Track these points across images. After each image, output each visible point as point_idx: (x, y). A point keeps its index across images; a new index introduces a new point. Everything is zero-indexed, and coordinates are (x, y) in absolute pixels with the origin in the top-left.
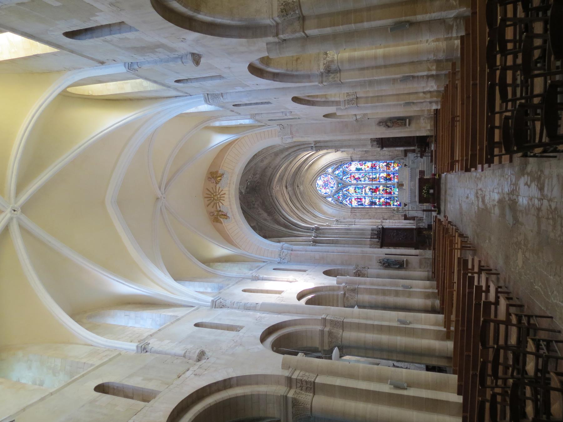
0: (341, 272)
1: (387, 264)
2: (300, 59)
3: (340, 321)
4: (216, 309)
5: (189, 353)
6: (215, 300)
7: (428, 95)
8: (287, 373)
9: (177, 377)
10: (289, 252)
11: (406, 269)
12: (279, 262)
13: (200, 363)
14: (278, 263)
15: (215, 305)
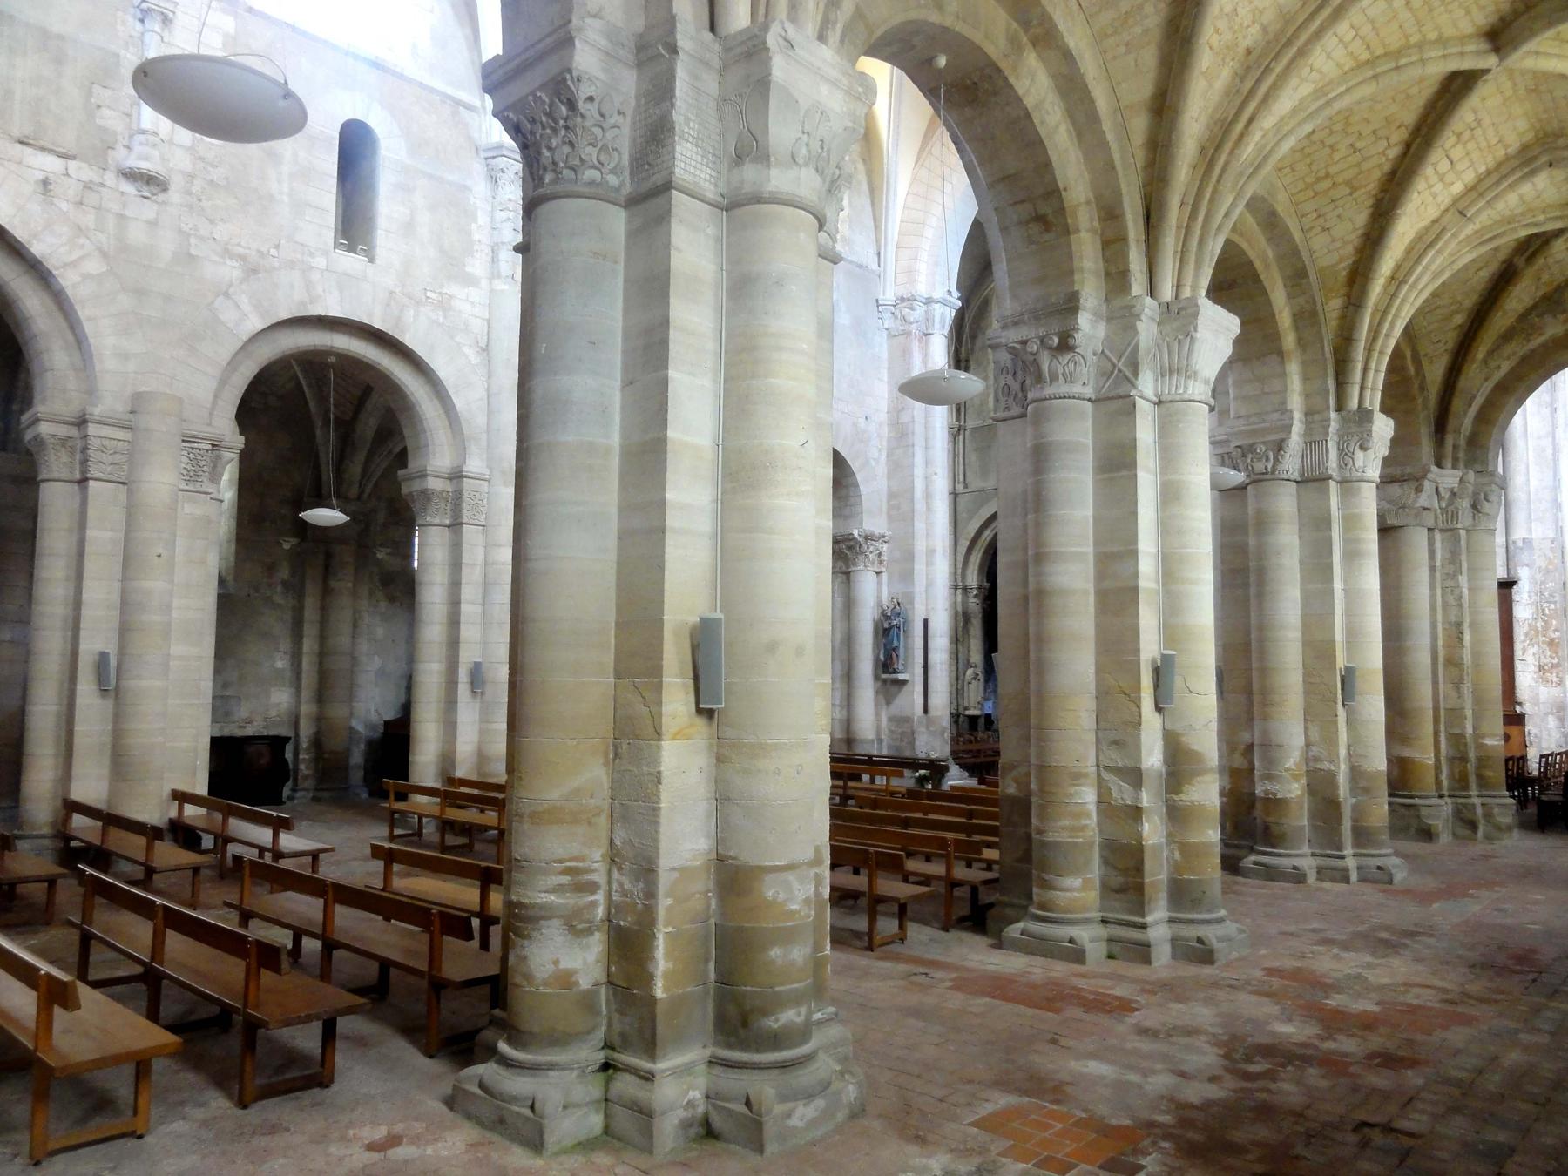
0: (851, 494)
1: (886, 626)
2: (1048, 230)
3: (461, 517)
4: (483, 161)
5: (141, 144)
6: (505, 153)
7: (1239, 762)
8: (109, 403)
9: (16, 133)
10: (914, 325)
11: (876, 677)
12: (880, 302)
13: (110, 178)
14: (877, 301)
15: (494, 157)
